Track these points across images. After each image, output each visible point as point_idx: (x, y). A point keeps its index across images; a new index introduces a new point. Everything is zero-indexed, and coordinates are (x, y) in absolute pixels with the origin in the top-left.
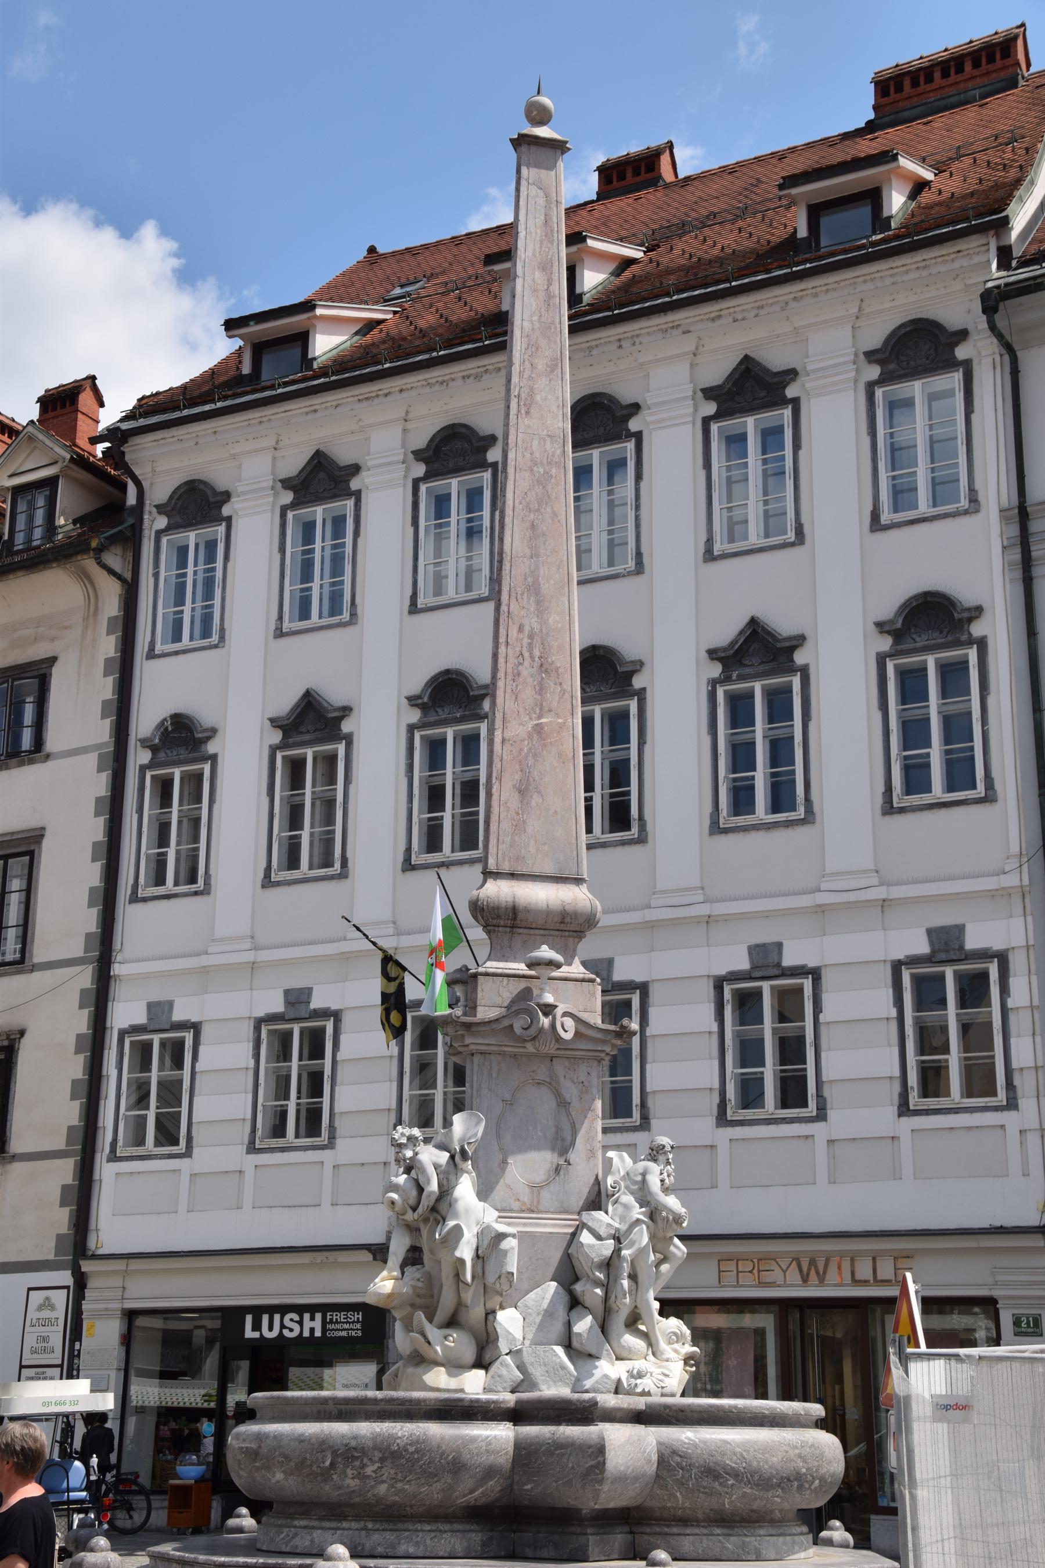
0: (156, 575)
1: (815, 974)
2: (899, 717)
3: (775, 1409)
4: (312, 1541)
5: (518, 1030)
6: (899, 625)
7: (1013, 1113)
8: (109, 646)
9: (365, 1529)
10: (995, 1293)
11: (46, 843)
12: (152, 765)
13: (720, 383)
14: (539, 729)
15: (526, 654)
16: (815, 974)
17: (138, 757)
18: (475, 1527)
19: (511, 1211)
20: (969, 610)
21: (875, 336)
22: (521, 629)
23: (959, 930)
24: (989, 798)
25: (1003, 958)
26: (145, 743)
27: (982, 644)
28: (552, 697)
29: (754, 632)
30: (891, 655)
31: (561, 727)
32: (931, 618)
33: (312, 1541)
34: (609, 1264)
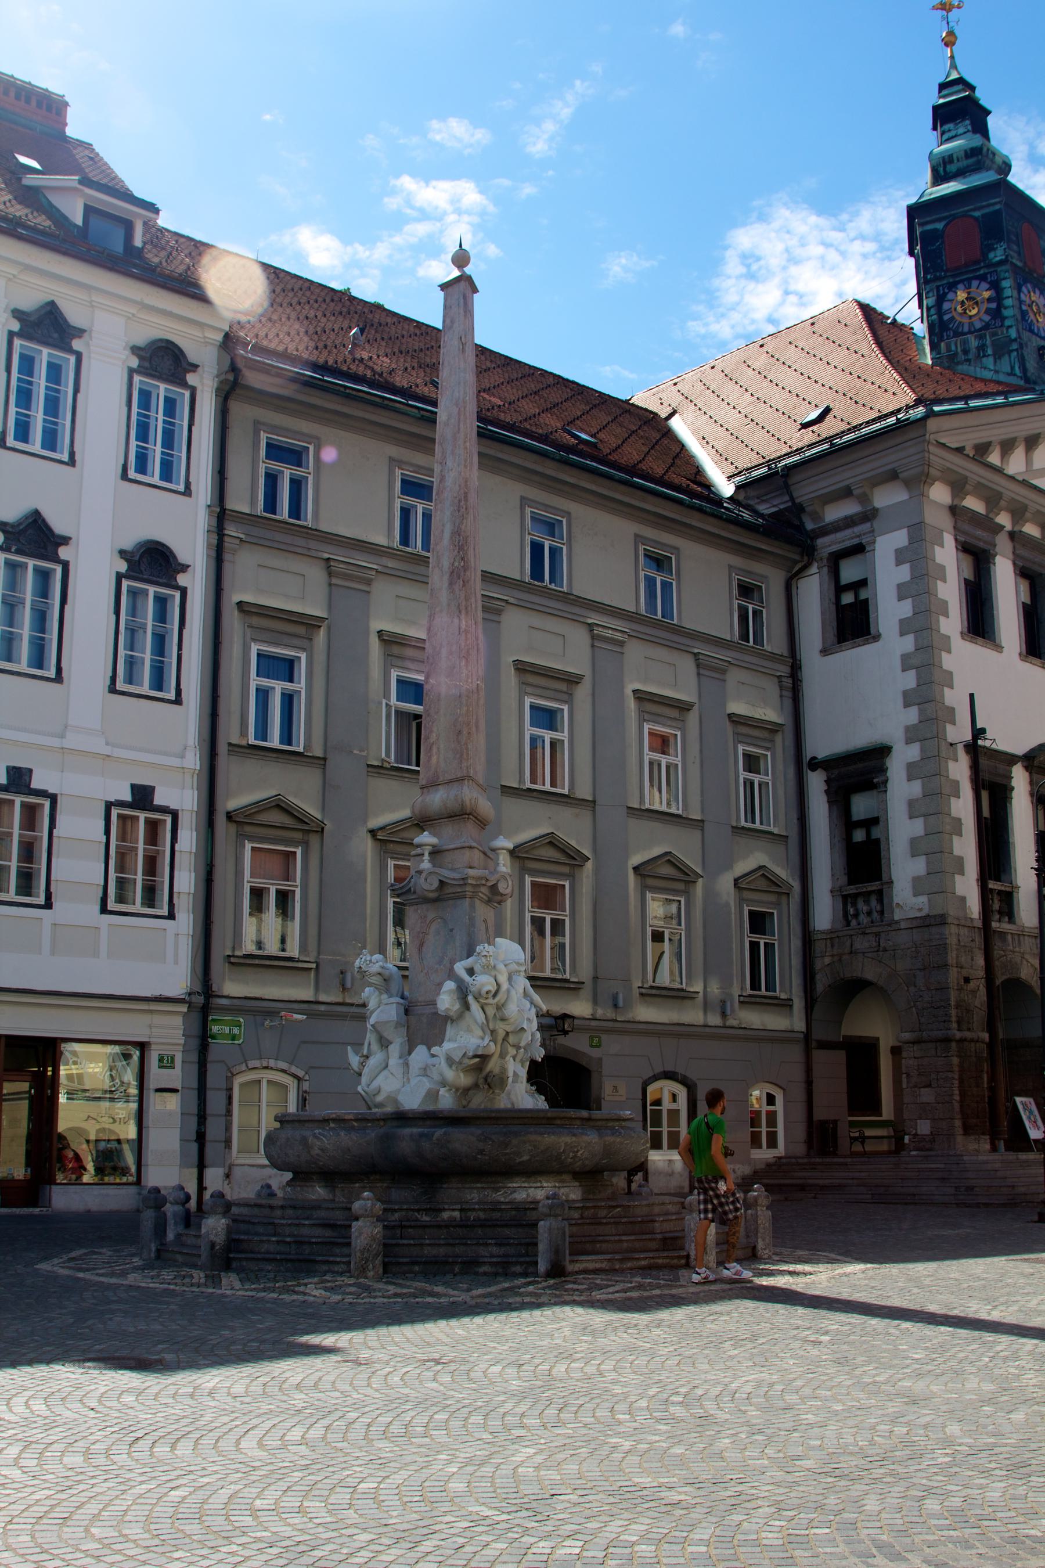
1: (53, 799)
4: (528, 1195)
6: (137, 558)
10: (152, 1040)
13: (72, 324)
18: (577, 1184)
20: (183, 565)
21: (143, 336)
23: (152, 789)
24: (178, 701)
25: (175, 815)
27: (184, 592)
29: (35, 521)
30: (127, 576)
32: (152, 562)
33: (528, 1195)
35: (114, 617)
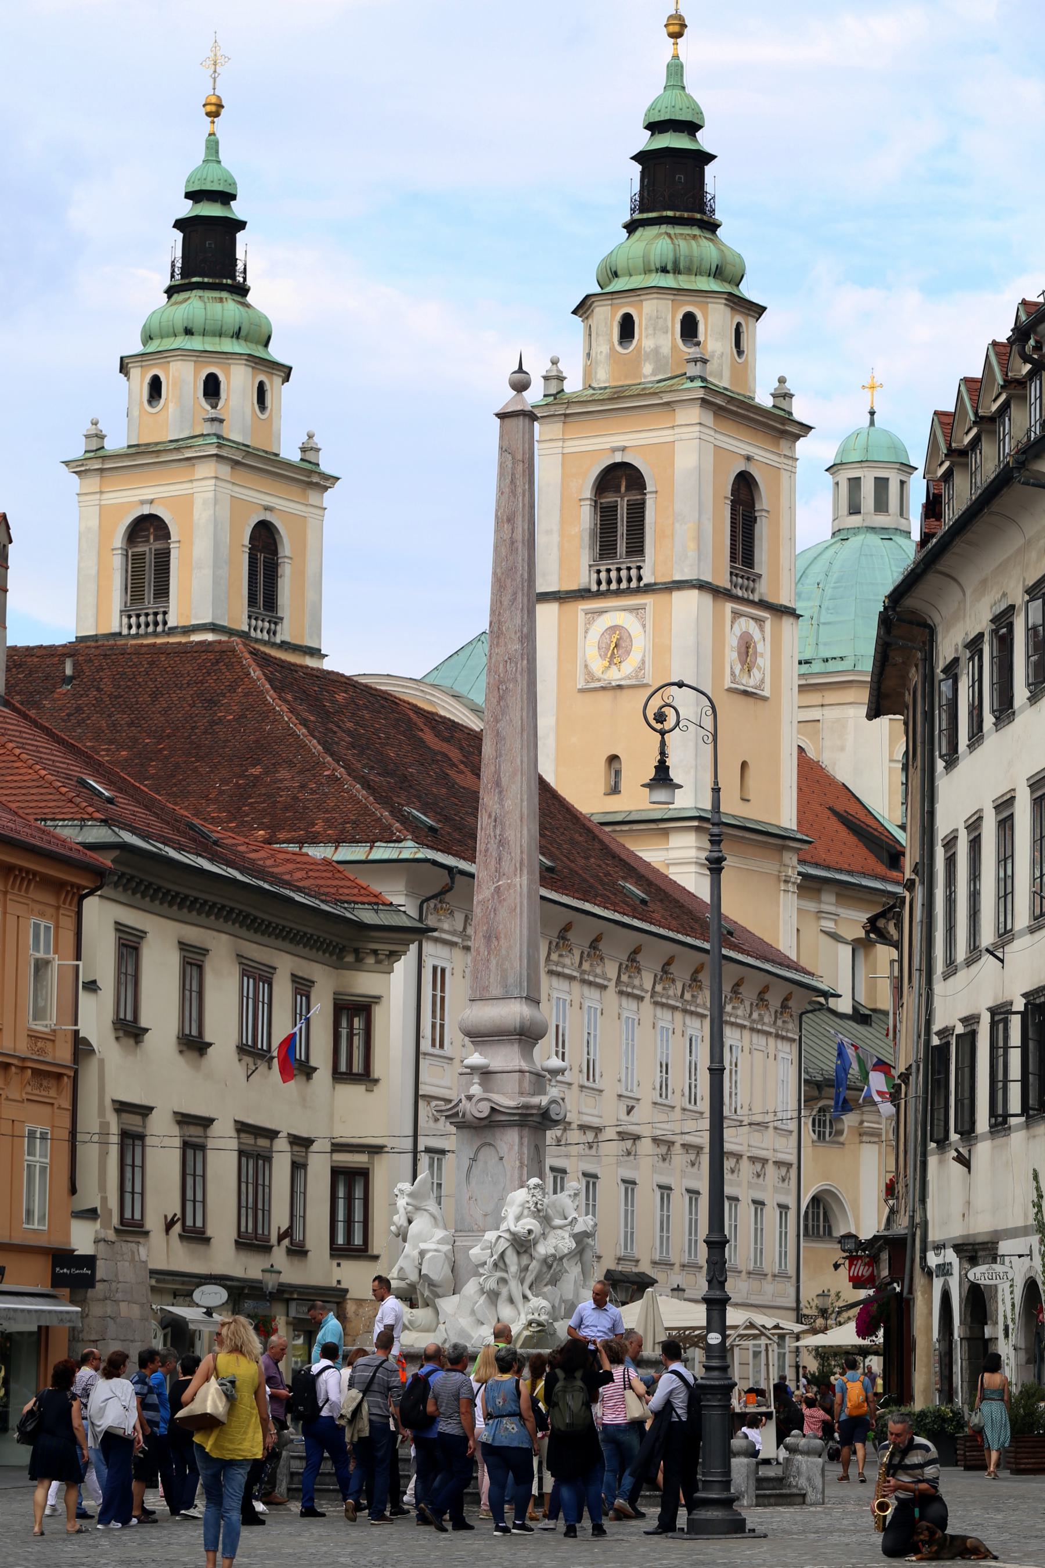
14: (498, 888)
15: (492, 834)
22: (490, 816)
28: (506, 866)
31: (509, 886)
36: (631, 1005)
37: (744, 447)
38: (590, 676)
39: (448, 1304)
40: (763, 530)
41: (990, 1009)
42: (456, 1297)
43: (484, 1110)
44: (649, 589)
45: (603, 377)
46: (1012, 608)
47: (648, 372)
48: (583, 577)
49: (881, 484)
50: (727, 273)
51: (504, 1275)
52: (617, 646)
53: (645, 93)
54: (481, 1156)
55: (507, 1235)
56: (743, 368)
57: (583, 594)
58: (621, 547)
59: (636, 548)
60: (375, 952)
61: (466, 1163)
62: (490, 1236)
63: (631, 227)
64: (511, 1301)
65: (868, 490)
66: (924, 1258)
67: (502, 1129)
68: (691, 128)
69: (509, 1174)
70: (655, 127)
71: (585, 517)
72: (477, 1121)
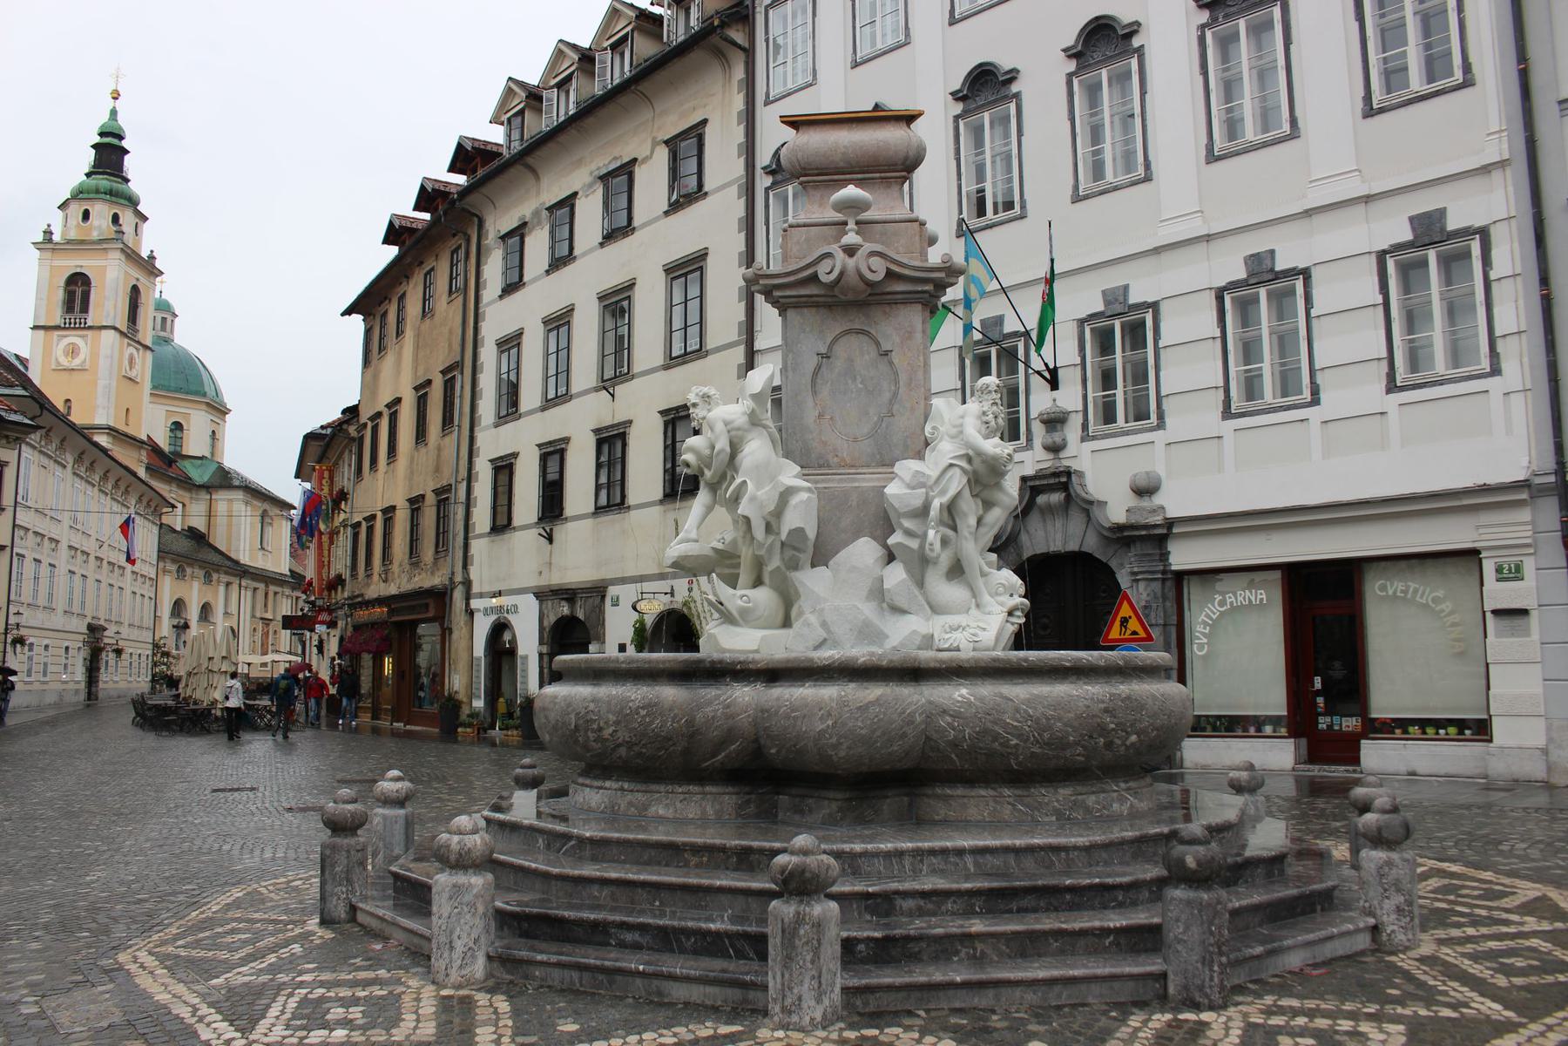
0: (767, 41)
2: (1376, 26)
3: (1080, 659)
5: (824, 278)
7: (1497, 379)
8: (739, 102)
9: (622, 789)
11: (709, 259)
12: (774, 184)
16: (1306, 274)
17: (763, 181)
18: (730, 789)
19: (829, 466)
23: (1441, 213)
25: (1484, 233)
26: (769, 171)
34: (923, 512)
35: (1356, 25)
36: (102, 496)
37: (136, 274)
38: (58, 363)
39: (813, 581)
40: (141, 311)
41: (596, 431)
42: (821, 570)
43: (878, 269)
44: (90, 328)
45: (73, 235)
46: (635, 160)
47: (95, 235)
48: (58, 321)
49: (164, 320)
50: (132, 202)
51: (950, 533)
52: (73, 351)
53: (104, 118)
54: (841, 350)
55: (964, 464)
56: (138, 243)
57: (57, 328)
58: (77, 308)
59: (85, 309)
60: (7, 437)
61: (811, 363)
62: (907, 468)
63: (88, 175)
64: (957, 571)
65: (159, 320)
66: (468, 604)
67: (887, 309)
68: (121, 138)
69: (903, 377)
70: (101, 134)
71: (60, 295)
72: (862, 285)
